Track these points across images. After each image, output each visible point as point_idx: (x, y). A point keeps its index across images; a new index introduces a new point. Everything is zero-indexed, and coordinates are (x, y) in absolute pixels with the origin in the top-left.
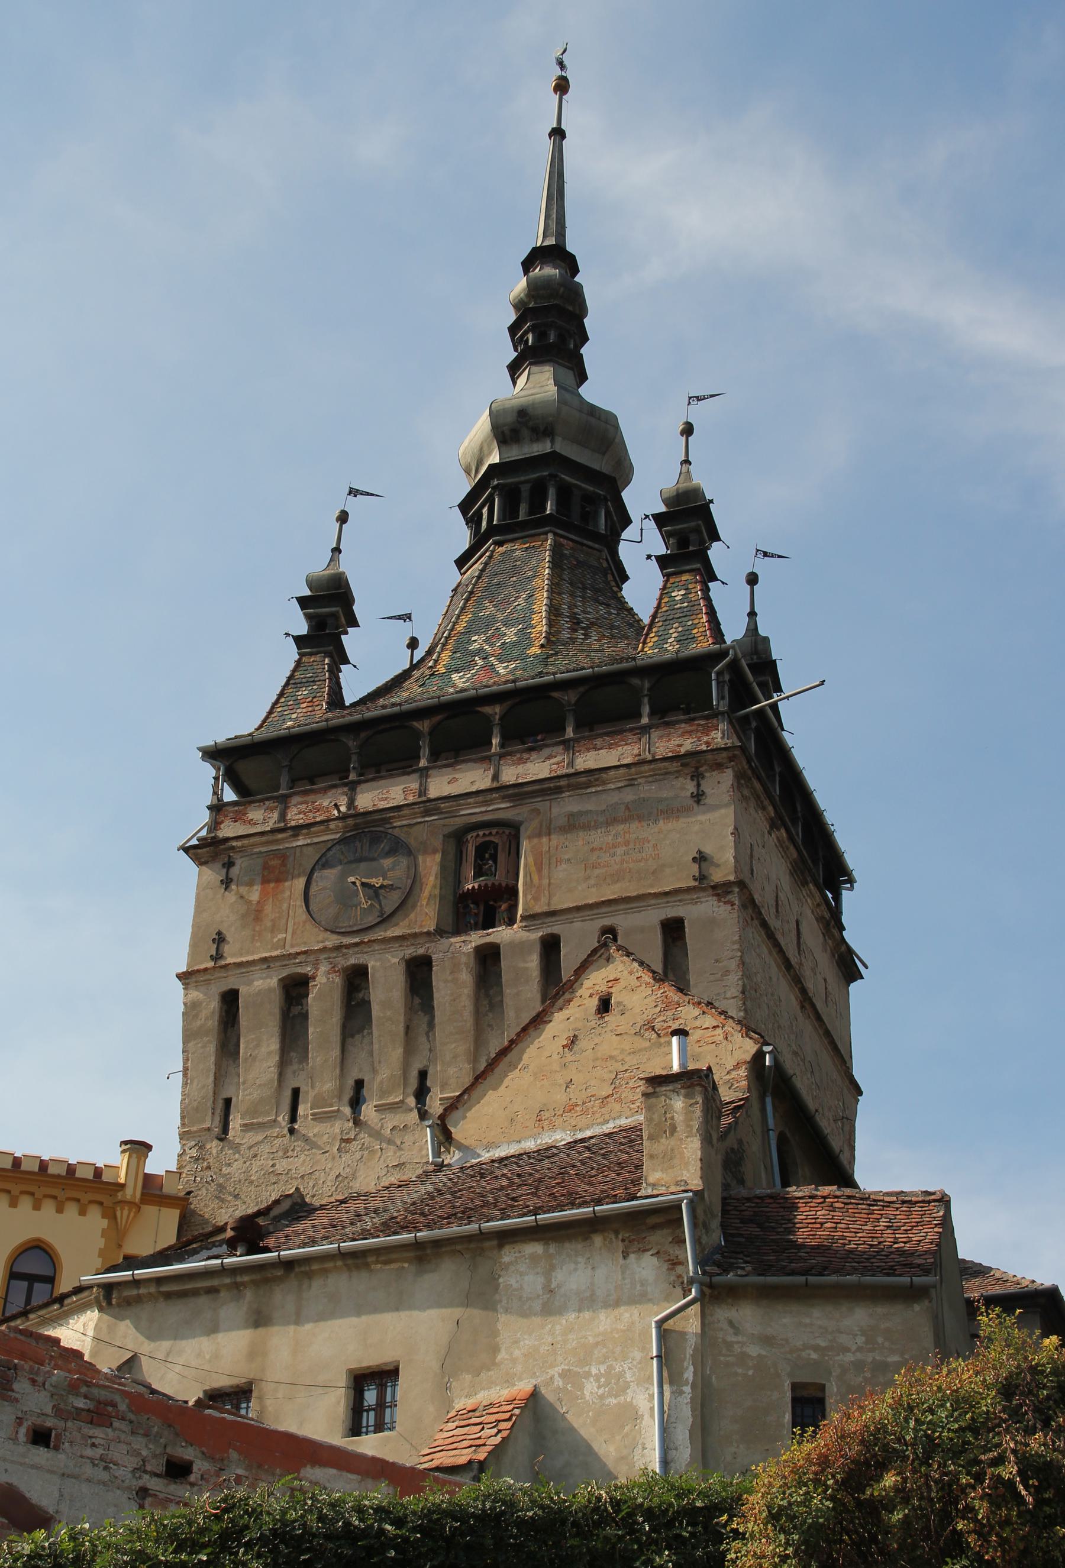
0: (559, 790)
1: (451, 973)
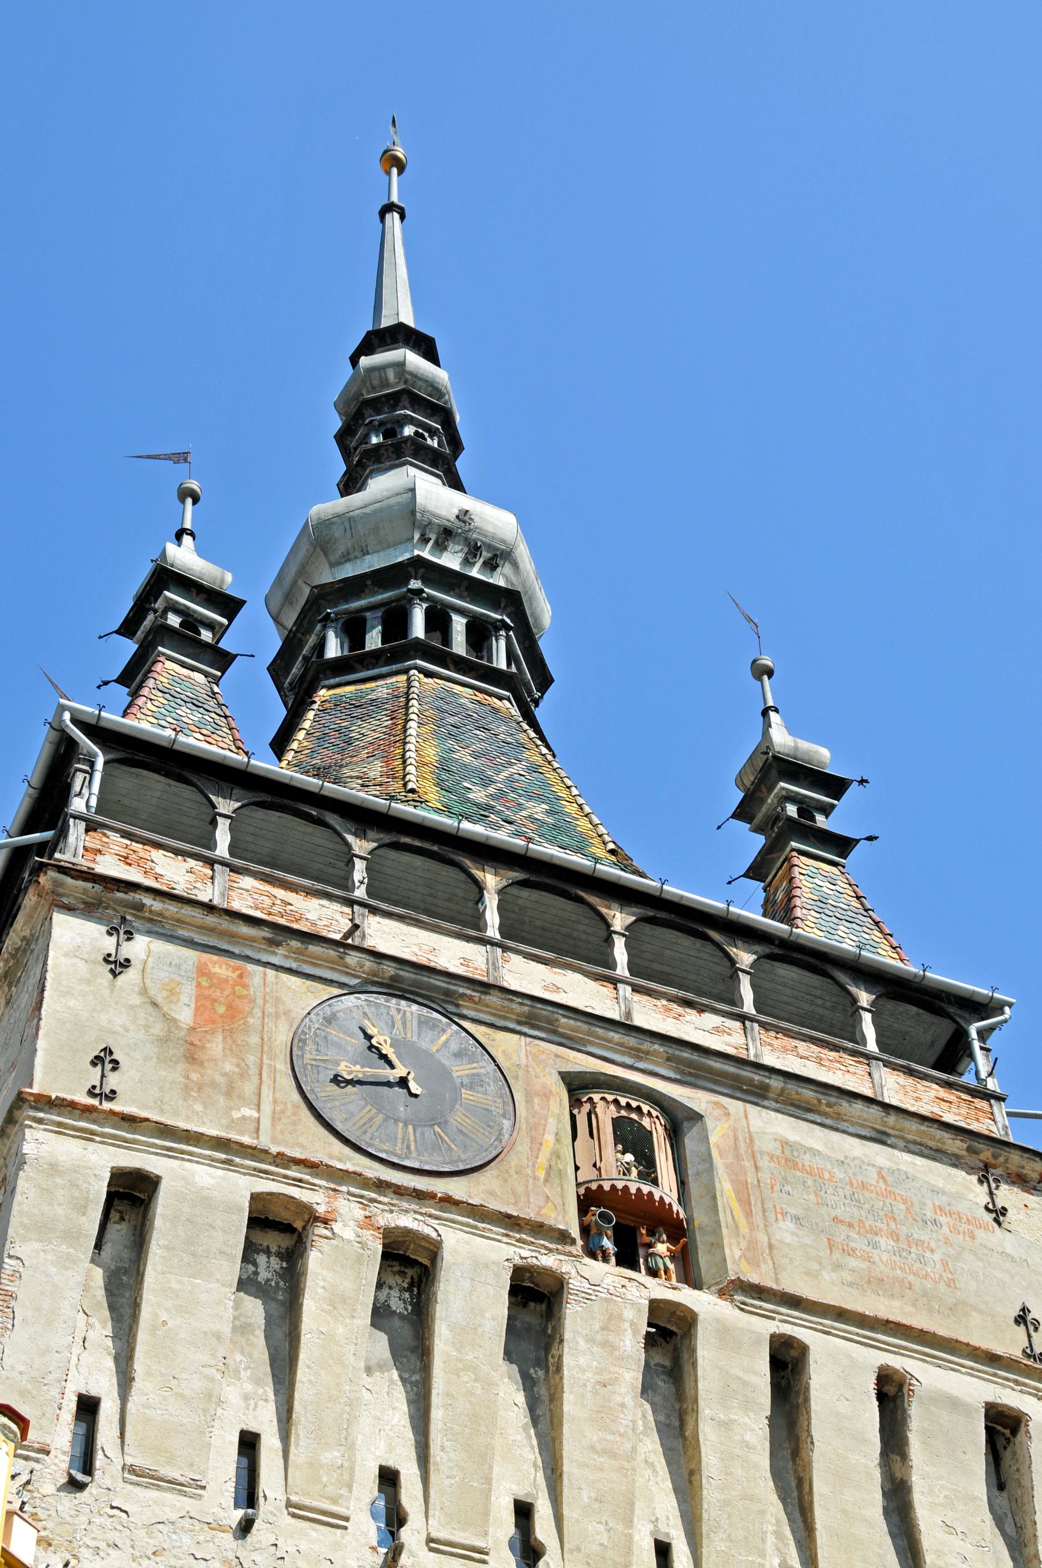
1: (602, 1329)
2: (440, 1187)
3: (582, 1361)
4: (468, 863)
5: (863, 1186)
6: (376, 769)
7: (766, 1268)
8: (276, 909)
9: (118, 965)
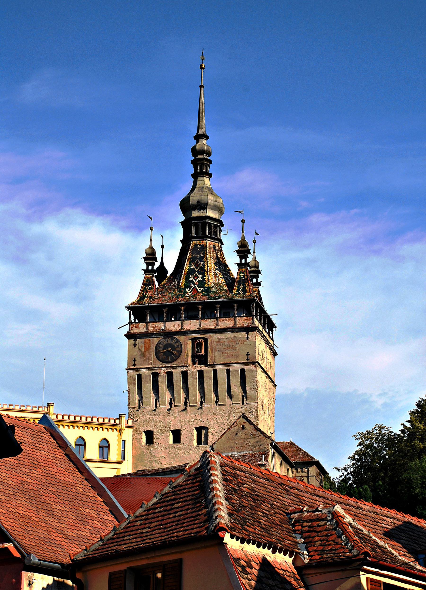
1: (192, 376)
3: (190, 380)
9: (135, 345)
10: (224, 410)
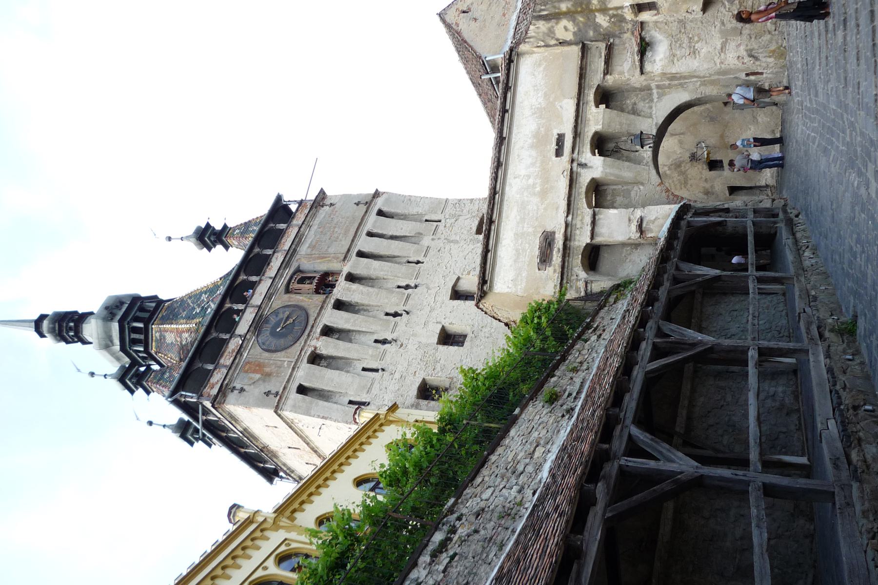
0: (295, 250)
1: (350, 291)
2: (311, 322)
4: (223, 310)
5: (322, 232)
6: (185, 335)
7: (340, 255)
8: (231, 355)
10: (438, 250)
